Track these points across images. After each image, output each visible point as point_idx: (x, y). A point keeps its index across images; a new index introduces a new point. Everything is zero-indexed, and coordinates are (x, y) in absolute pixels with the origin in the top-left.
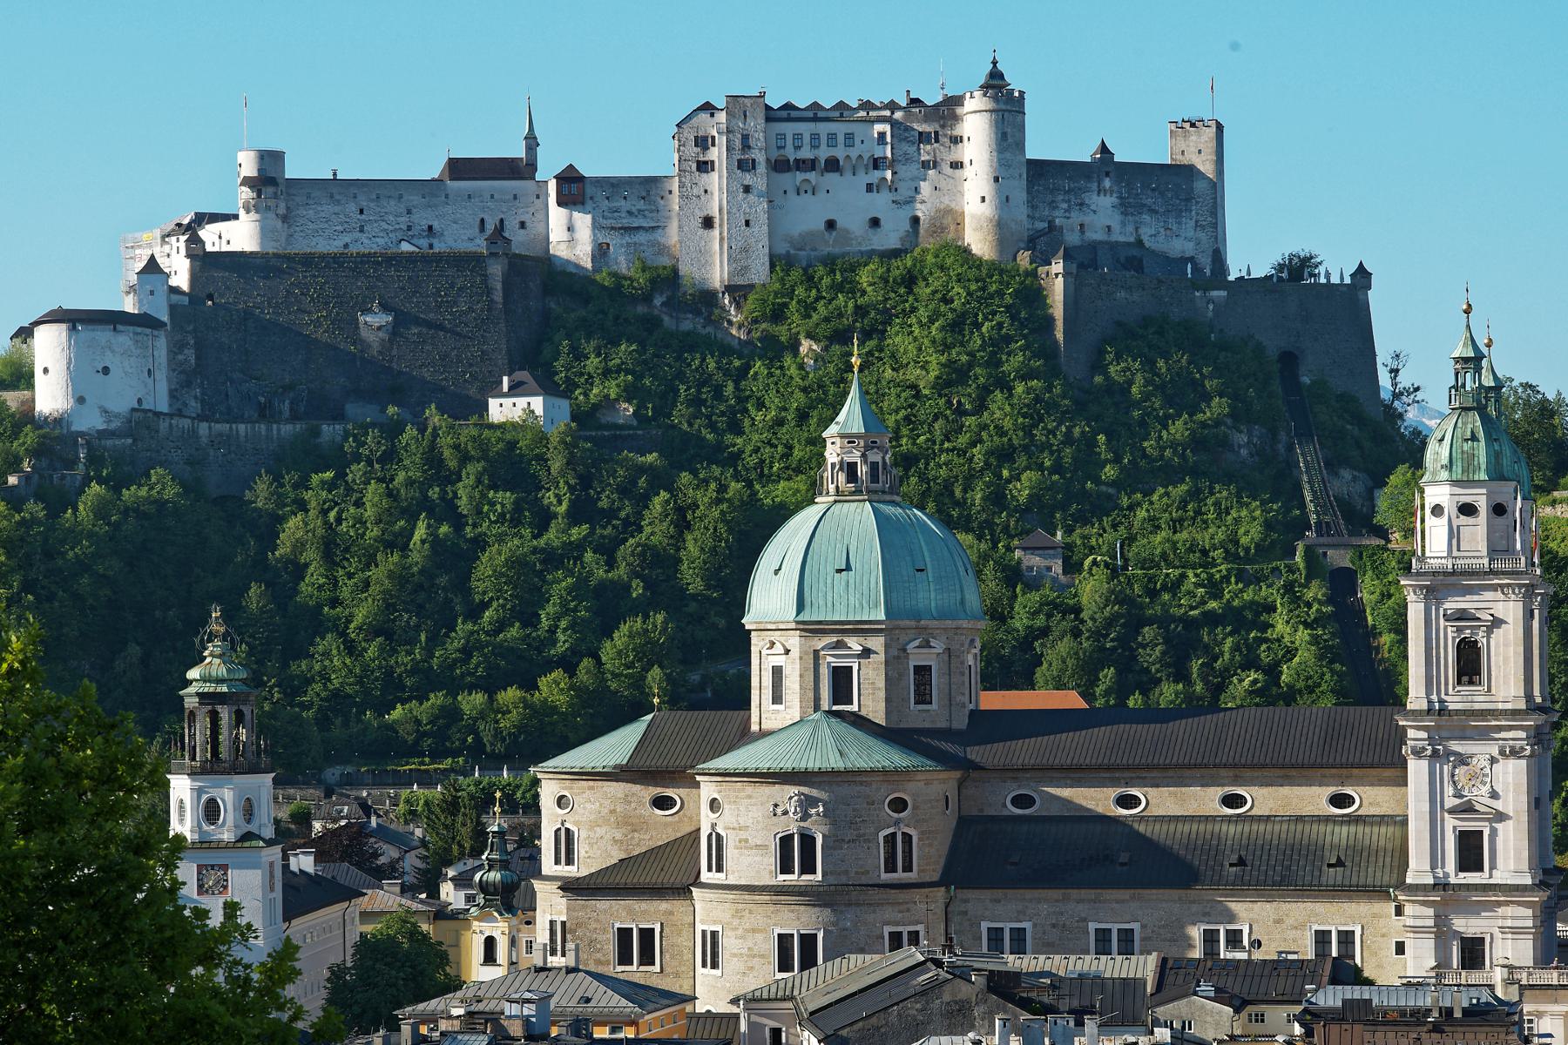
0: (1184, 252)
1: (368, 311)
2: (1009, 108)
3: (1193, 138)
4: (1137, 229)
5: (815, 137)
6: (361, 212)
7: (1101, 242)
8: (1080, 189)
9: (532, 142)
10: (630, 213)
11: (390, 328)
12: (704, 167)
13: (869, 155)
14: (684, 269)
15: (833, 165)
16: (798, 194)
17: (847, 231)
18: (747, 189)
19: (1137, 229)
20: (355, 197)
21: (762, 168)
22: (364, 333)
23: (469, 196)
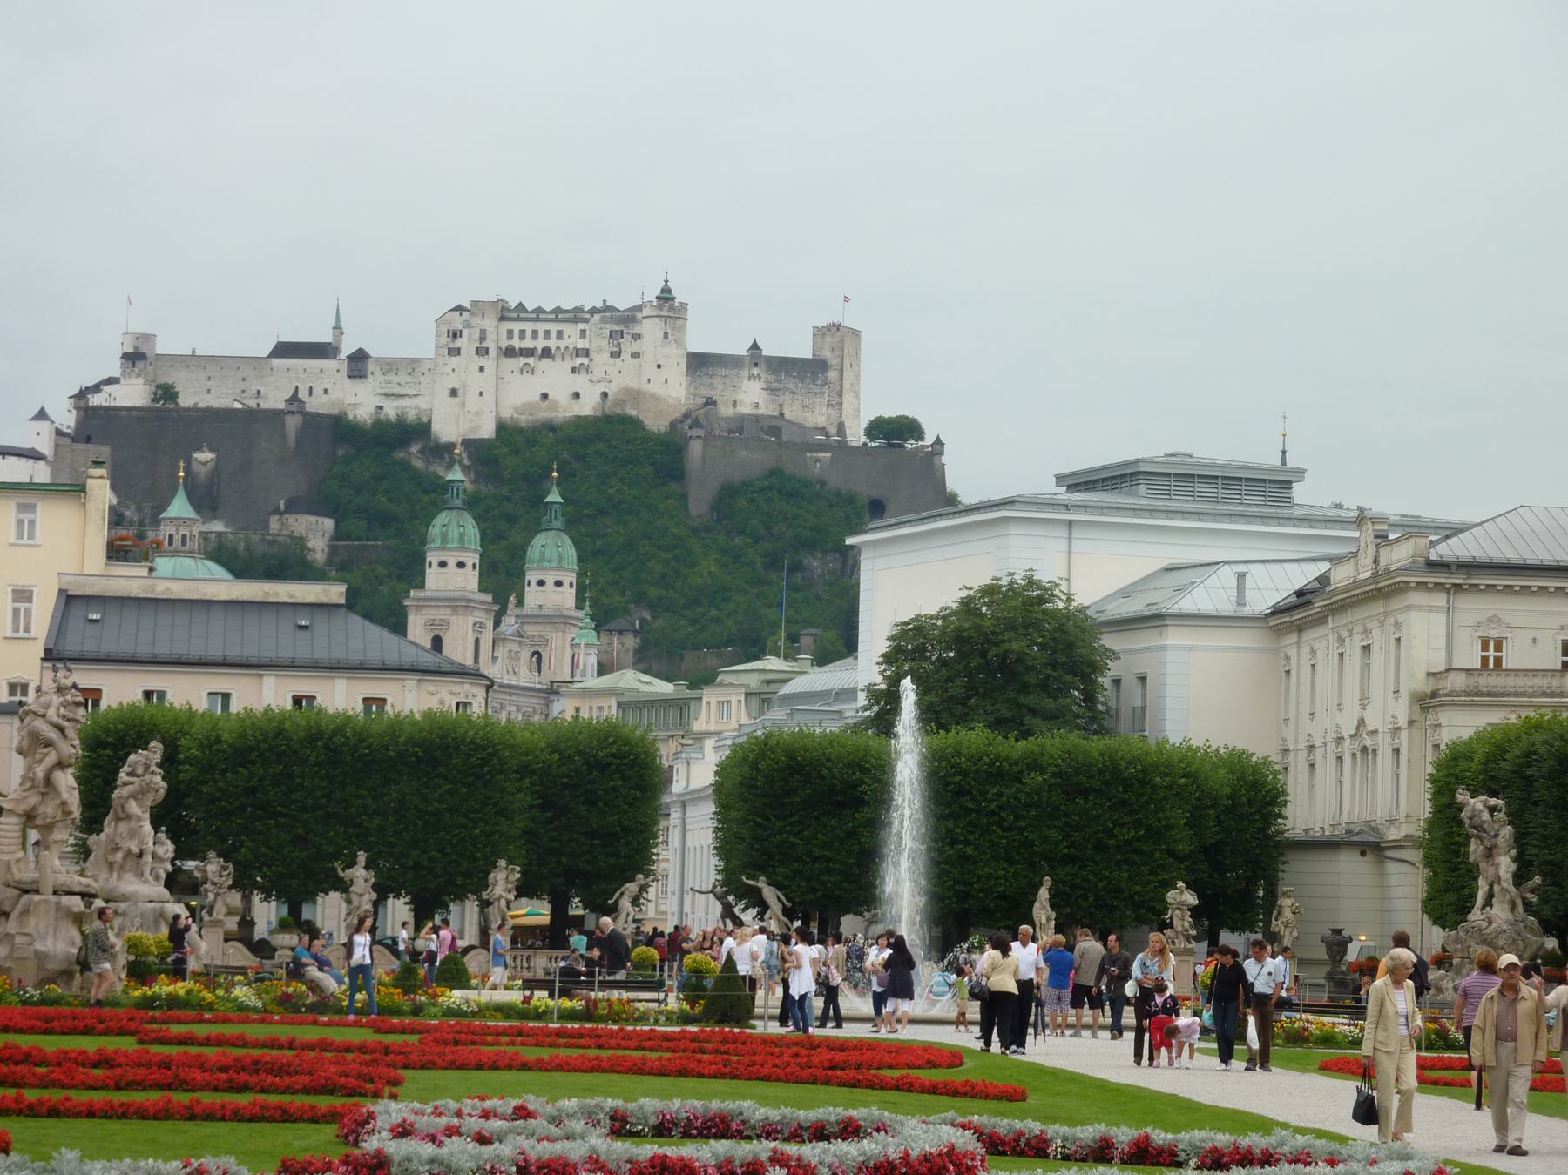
0: (817, 423)
1: (199, 449)
2: (671, 314)
3: (829, 339)
5: (535, 334)
6: (209, 379)
7: (749, 415)
9: (337, 327)
10: (399, 384)
11: (213, 463)
14: (435, 427)
15: (546, 353)
17: (556, 402)
18: (482, 369)
19: (781, 405)
20: (205, 367)
21: (492, 352)
22: (195, 467)
23: (288, 370)
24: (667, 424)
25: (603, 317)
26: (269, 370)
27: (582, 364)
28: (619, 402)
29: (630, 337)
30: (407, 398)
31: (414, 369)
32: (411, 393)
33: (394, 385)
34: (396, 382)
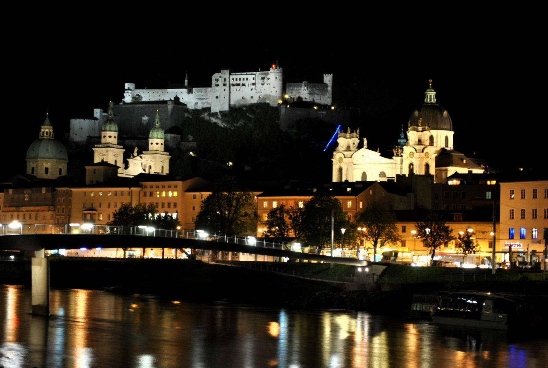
1: (143, 116)
2: (277, 71)
3: (328, 78)
4: (313, 99)
5: (240, 79)
8: (299, 89)
10: (202, 96)
11: (148, 120)
12: (217, 85)
14: (212, 108)
15: (243, 85)
18: (225, 90)
19: (313, 99)
20: (149, 93)
21: (228, 85)
22: (143, 122)
24: (277, 104)
25: (259, 73)
26: (166, 93)
28: (264, 99)
29: (267, 79)
30: (204, 100)
31: (206, 91)
33: (201, 96)
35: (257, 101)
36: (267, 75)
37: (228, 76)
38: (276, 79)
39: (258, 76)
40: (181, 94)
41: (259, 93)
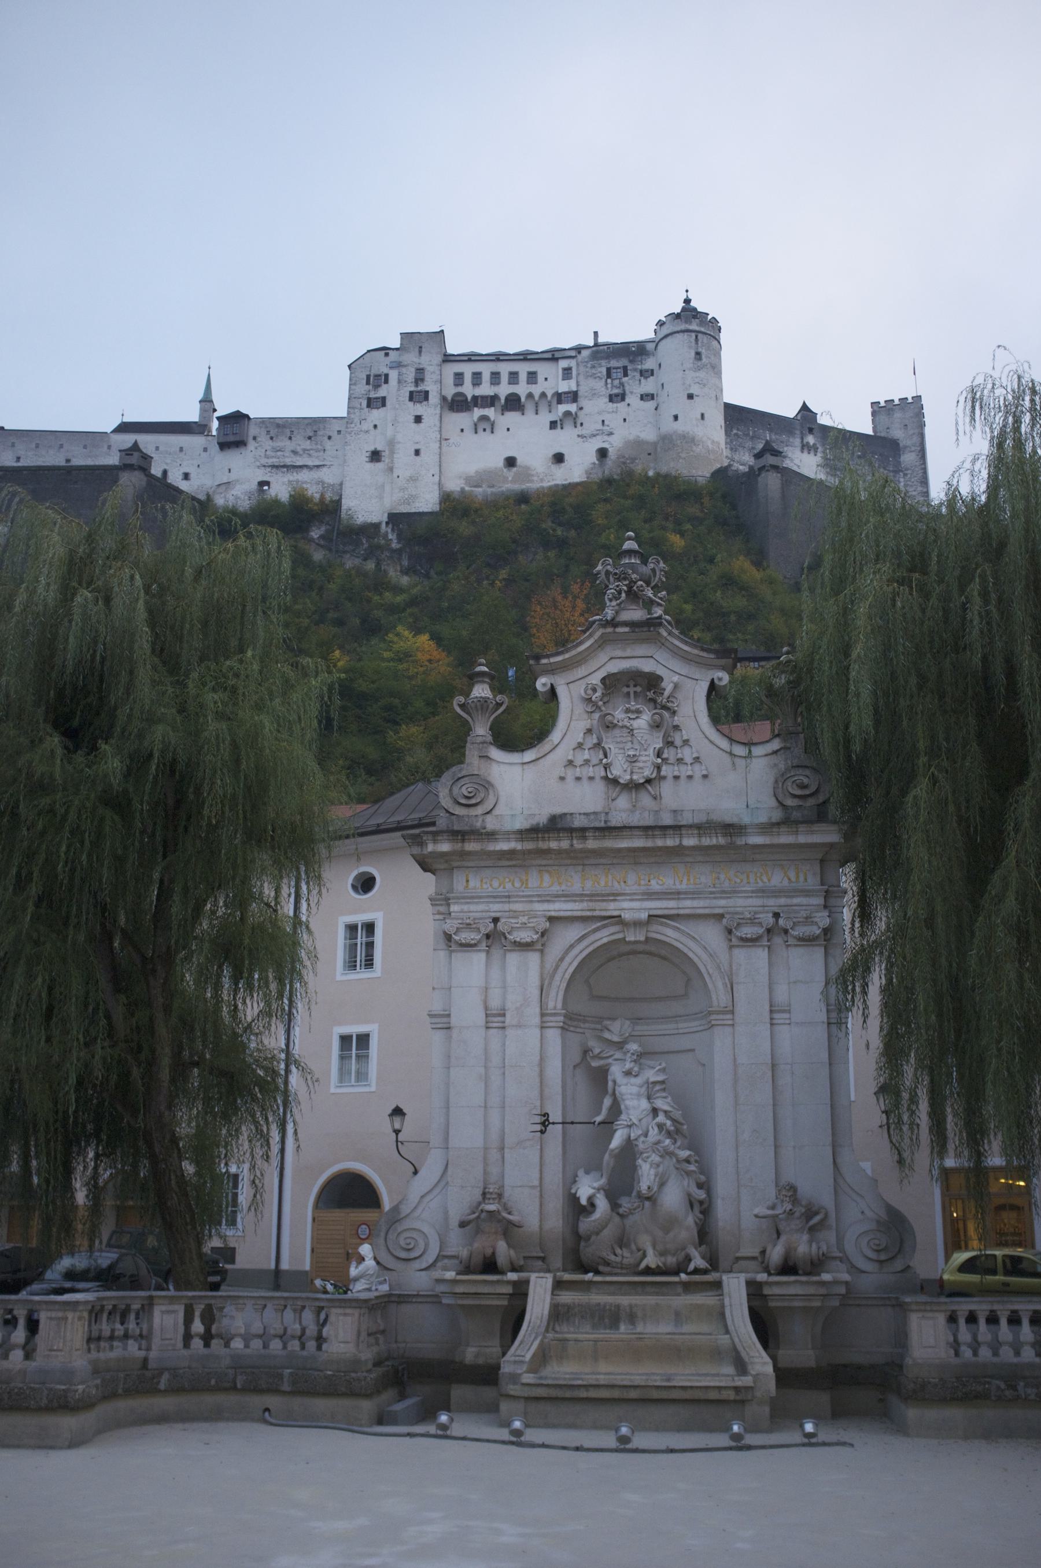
2: (703, 329)
3: (898, 415)
5: (495, 377)
9: (207, 401)
10: (295, 452)
13: (555, 390)
14: (346, 503)
15: (513, 403)
16: (476, 433)
17: (528, 468)
18: (418, 419)
20: (13, 445)
21: (434, 398)
24: (708, 475)
26: (106, 447)
27: (568, 414)
29: (637, 375)
30: (305, 471)
32: (310, 463)
33: (287, 454)
34: (287, 449)
35: (588, 473)
36: (639, 358)
37: (439, 358)
38: (699, 363)
39: (589, 365)
40: (181, 455)
41: (598, 437)
